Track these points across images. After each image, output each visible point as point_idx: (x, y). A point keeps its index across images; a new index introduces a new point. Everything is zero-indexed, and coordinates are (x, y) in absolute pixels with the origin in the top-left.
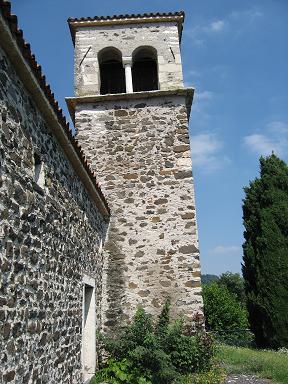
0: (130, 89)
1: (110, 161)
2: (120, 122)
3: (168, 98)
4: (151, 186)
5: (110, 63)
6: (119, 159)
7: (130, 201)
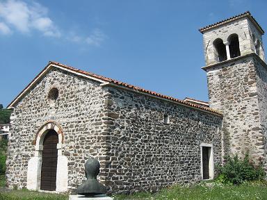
0: (229, 58)
1: (222, 93)
2: (224, 74)
3: (244, 59)
4: (239, 102)
5: (219, 44)
6: (225, 91)
7: (231, 109)
